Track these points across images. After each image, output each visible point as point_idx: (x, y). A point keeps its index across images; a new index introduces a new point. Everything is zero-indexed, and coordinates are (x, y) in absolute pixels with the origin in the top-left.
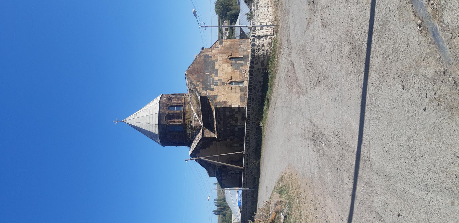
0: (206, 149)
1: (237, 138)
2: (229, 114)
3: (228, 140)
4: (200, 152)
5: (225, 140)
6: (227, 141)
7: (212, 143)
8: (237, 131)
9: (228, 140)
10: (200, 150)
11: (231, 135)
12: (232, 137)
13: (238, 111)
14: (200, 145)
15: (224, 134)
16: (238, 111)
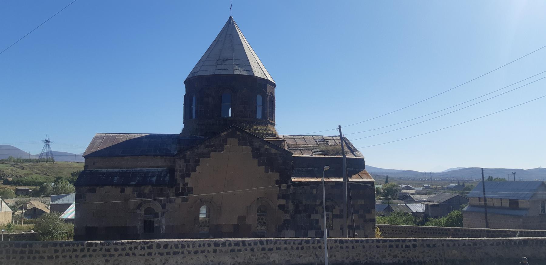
0: (254, 158)
1: (289, 218)
2: (359, 203)
3: (283, 202)
4: (244, 147)
5: (284, 196)
6: (279, 198)
7: (272, 172)
8: (309, 217)
9: (283, 202)
10: (250, 149)
11: (297, 207)
12: (291, 207)
13: (366, 218)
14: (266, 149)
15: (301, 193)
16: (366, 218)
